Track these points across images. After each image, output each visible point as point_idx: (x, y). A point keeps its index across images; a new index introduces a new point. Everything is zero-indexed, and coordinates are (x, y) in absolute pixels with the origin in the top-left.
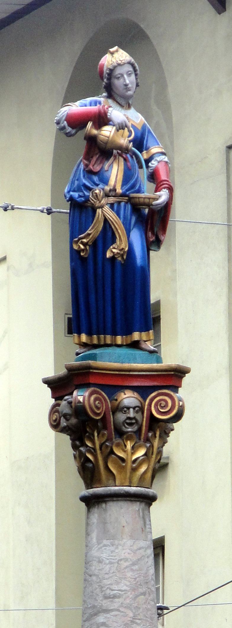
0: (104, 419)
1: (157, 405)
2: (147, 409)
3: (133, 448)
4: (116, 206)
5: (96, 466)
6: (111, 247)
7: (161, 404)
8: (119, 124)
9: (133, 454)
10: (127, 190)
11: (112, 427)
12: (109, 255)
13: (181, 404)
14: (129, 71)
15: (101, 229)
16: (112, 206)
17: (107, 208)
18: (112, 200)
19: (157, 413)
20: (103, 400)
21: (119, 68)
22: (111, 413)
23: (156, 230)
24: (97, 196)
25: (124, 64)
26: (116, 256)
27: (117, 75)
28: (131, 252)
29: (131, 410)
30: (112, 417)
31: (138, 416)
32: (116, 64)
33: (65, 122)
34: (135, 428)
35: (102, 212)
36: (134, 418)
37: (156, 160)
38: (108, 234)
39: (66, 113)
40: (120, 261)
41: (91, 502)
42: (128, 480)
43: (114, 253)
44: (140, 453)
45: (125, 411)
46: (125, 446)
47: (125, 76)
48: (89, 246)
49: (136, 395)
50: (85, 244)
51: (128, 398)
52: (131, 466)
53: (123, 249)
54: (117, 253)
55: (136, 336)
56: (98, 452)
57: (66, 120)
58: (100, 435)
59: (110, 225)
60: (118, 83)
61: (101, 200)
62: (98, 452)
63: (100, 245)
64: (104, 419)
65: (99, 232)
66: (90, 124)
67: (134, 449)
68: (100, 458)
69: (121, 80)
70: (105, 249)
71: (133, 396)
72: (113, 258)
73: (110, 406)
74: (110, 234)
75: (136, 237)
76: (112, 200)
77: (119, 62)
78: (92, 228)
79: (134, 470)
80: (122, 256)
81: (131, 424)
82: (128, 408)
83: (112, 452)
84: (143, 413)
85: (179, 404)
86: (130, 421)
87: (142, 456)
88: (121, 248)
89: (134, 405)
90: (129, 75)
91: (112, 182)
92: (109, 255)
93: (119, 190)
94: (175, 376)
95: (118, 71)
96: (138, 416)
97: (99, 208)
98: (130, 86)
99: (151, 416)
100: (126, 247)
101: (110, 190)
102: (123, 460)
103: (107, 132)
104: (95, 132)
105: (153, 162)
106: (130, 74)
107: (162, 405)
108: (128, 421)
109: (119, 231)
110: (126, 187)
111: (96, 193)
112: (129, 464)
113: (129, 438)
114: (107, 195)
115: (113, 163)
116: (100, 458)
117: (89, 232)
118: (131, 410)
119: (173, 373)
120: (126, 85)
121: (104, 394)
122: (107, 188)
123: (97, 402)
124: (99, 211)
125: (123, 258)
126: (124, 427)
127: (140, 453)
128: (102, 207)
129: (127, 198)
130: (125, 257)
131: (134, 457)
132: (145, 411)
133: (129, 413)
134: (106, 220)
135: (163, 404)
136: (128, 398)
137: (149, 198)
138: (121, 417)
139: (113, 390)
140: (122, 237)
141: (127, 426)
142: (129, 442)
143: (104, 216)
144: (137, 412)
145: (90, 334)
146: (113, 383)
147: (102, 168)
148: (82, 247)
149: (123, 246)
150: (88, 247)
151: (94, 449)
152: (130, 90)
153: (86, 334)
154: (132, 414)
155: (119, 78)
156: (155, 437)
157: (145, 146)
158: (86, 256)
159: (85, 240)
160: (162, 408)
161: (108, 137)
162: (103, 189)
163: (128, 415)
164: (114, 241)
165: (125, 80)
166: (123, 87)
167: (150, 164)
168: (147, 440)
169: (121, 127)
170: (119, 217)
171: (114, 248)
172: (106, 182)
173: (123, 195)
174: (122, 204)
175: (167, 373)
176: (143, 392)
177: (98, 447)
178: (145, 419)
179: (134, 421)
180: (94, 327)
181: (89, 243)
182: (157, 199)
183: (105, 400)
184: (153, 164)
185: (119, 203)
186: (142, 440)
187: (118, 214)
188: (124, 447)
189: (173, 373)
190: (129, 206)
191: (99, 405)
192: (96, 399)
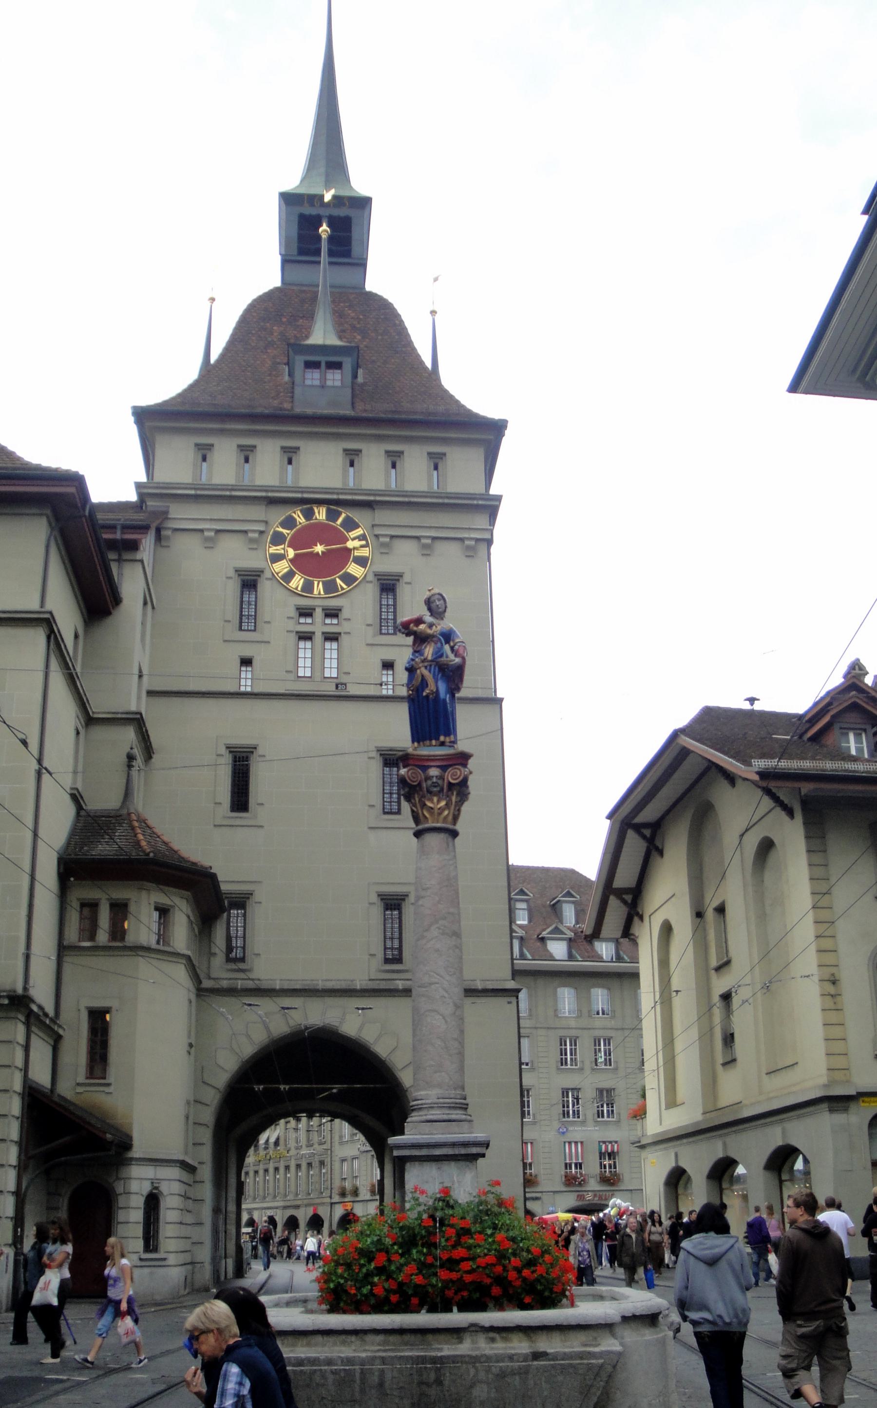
0: (420, 784)
5: (418, 814)
12: (424, 694)
16: (426, 667)
18: (426, 664)
31: (440, 782)
44: (443, 803)
60: (433, 606)
64: (420, 784)
66: (412, 625)
67: (439, 802)
70: (423, 691)
76: (426, 664)
79: (440, 814)
81: (435, 787)
83: (425, 805)
86: (435, 785)
90: (439, 600)
91: (426, 654)
92: (424, 694)
93: (430, 658)
95: (432, 599)
96: (440, 782)
102: (432, 808)
103: (422, 627)
112: (436, 811)
124: (418, 671)
127: (443, 803)
128: (420, 668)
131: (439, 806)
134: (423, 676)
138: (429, 782)
139: (425, 768)
146: (422, 764)
154: (434, 780)
168: (448, 796)
169: (431, 626)
172: (422, 655)
173: (431, 661)
176: (444, 768)
184: (456, 647)
185: (431, 666)
187: (430, 671)
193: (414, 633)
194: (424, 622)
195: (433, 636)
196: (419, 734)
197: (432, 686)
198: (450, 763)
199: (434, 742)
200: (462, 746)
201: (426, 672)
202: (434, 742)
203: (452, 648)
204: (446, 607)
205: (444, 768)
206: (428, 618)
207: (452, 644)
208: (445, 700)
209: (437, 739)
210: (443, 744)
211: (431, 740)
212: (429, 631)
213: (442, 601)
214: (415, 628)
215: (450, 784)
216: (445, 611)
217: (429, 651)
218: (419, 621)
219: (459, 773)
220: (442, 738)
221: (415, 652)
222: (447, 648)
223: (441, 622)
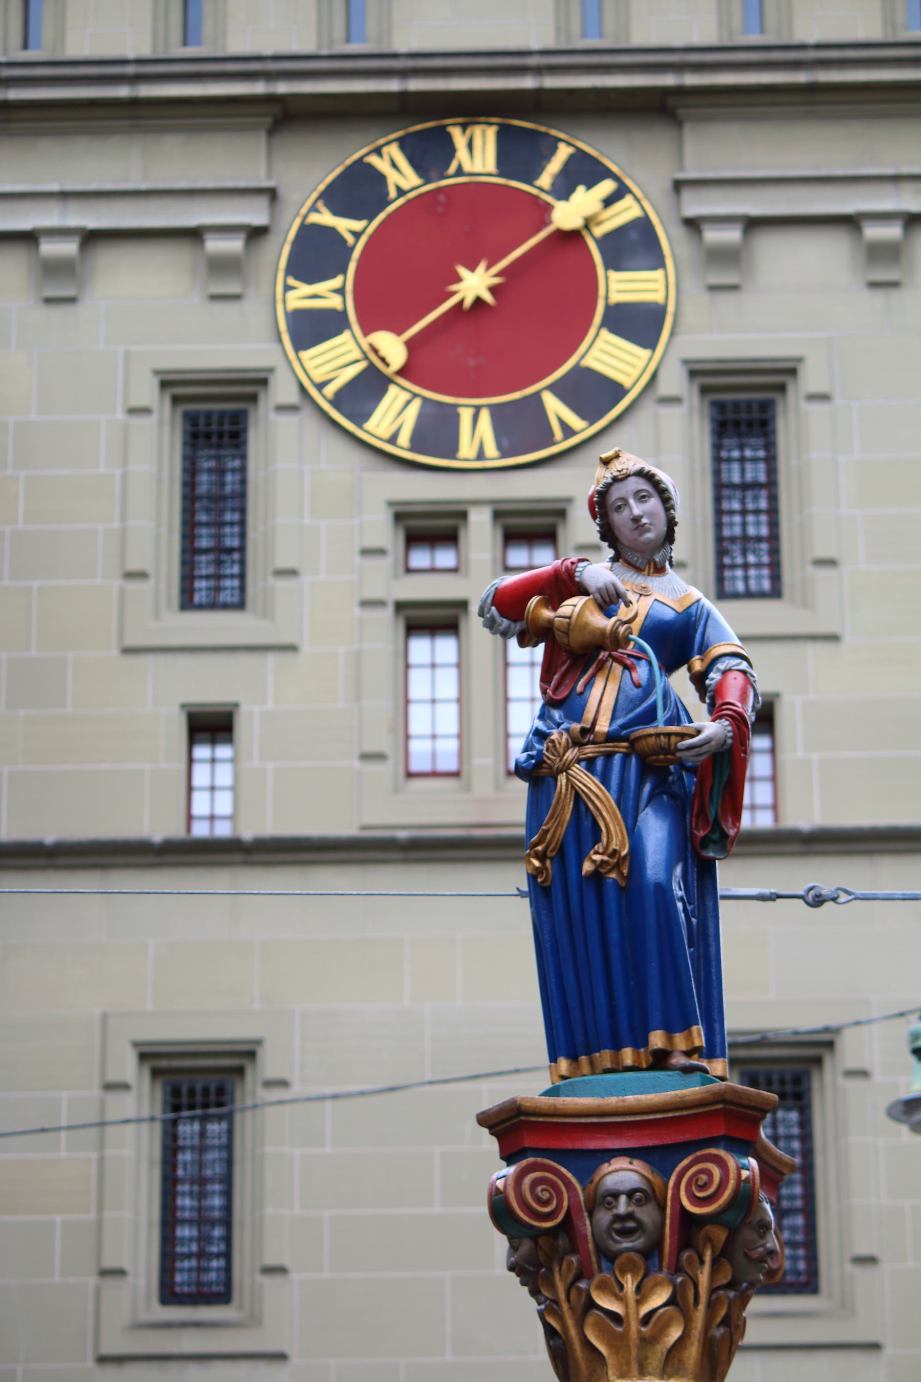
2: (673, 1195)
3: (638, 1289)
4: (599, 763)
6: (592, 852)
7: (697, 1181)
8: (599, 590)
9: (639, 1303)
10: (623, 727)
11: (591, 1246)
12: (587, 867)
13: (743, 1177)
14: (640, 491)
15: (568, 816)
16: (590, 764)
17: (578, 771)
18: (589, 750)
19: (693, 1204)
20: (560, 1183)
21: (616, 486)
22: (586, 1214)
23: (712, 813)
24: (554, 746)
25: (627, 476)
26: (603, 871)
27: (614, 503)
29: (623, 1199)
30: (588, 1223)
31: (647, 1214)
32: (610, 480)
33: (493, 608)
34: (638, 1242)
35: (568, 780)
36: (630, 1216)
37: (719, 670)
39: (493, 589)
40: (614, 879)
42: (634, 1366)
43: (594, 862)
44: (659, 1298)
45: (609, 1203)
46: (621, 1287)
47: (632, 501)
48: (551, 859)
49: (638, 1165)
50: (542, 857)
51: (622, 1174)
52: (639, 1332)
53: (615, 852)
54: (602, 861)
55: (657, 1039)
56: (565, 1306)
57: (494, 603)
58: (564, 1267)
59: (587, 808)
60: (620, 519)
61: (564, 755)
62: (565, 1306)
63: (571, 850)
64: (567, 1225)
65: (565, 825)
67: (642, 1293)
68: (570, 1323)
69: (625, 513)
70: (581, 857)
71: (630, 1167)
72: (597, 876)
73: (582, 1198)
74: (587, 823)
76: (589, 750)
77: (615, 474)
78: (550, 819)
79: (648, 1342)
80: (617, 866)
81: (626, 1233)
82: (616, 1195)
83: (591, 1305)
84: (662, 1208)
85: (739, 1175)
86: (626, 1226)
87: (664, 1305)
88: (610, 850)
89: (628, 1186)
90: (641, 497)
91: (589, 715)
92: (587, 867)
93: (603, 726)
95: (616, 493)
96: (647, 1214)
97: (560, 771)
98: (644, 520)
99: (683, 1208)
100: (623, 845)
101: (584, 732)
104: (547, 613)
105: (712, 675)
106: (644, 497)
107: (700, 1183)
108: (617, 1226)
109: (604, 813)
110: (620, 721)
111: (553, 741)
112: (634, 1326)
113: (629, 1267)
115: (594, 676)
116: (570, 1323)
117: (544, 827)
118: (623, 1199)
119: (720, 1106)
120: (636, 520)
121: (564, 1170)
122: (576, 727)
123: (539, 1188)
124: (562, 778)
125: (620, 873)
126: (610, 1242)
127: (659, 1298)
128: (566, 768)
129: (625, 744)
130: (625, 871)
131: (644, 1310)
132: (669, 1203)
133: (616, 1207)
135: (704, 1177)
136: (622, 1174)
137: (668, 735)
138: (604, 1217)
139: (587, 1162)
140: (611, 826)
141: (617, 1238)
142: (629, 1277)
143: (573, 787)
144: (639, 1203)
147: (574, 688)
148: (536, 863)
149: (614, 845)
150: (548, 863)
151: (556, 1302)
152: (648, 530)
153: (568, 1057)
154: (622, 1206)
155: (619, 507)
156: (702, 1262)
157: (696, 647)
158: (548, 884)
159: (540, 848)
160: (702, 1188)
161: (569, 618)
162: (567, 730)
163: (615, 1211)
164: (597, 839)
165: (631, 509)
166: (631, 525)
167: (708, 682)
168: (677, 1269)
170: (608, 788)
171: (597, 853)
172: (577, 716)
173: (610, 737)
174: (617, 757)
175: (706, 1109)
176: (660, 1158)
177: (562, 1296)
178: (668, 1222)
179: (631, 1224)
180: (580, 1038)
181: (549, 854)
182: (692, 736)
183: (568, 1184)
185: (609, 756)
186: (665, 1270)
188: (617, 1289)
189: (720, 1106)
190: (634, 760)
191: (545, 1196)
192: (535, 1183)
194: (581, 590)
195: (615, 641)
196: (574, 1028)
197: (615, 835)
198: (680, 1138)
199: (628, 1055)
201: (588, 782)
202: (628, 1055)
203: (699, 680)
204: (671, 523)
207: (698, 665)
208: (663, 890)
209: (640, 1042)
210: (660, 1061)
211: (617, 1047)
212: (599, 621)
213: (654, 503)
214: (547, 613)
215: (687, 1221)
216: (669, 537)
217: (602, 698)
219: (717, 1172)
220: (657, 1039)
221: (550, 703)
222: (680, 683)
223: (654, 583)
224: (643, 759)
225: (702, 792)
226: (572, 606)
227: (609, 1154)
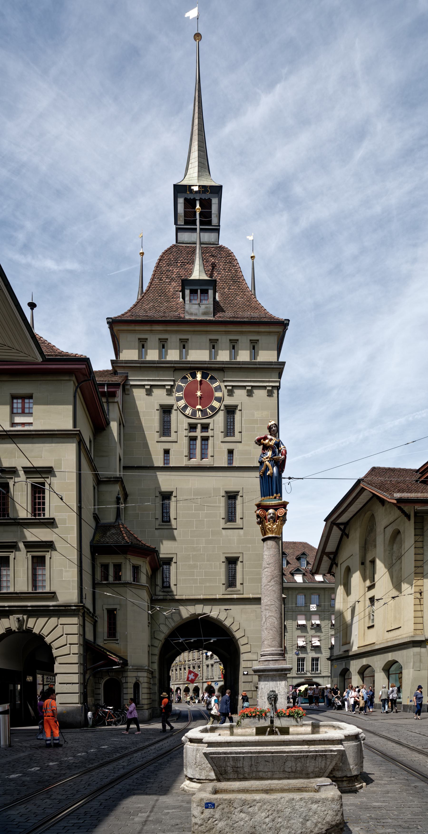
1: (280, 512)
12: (267, 474)
16: (268, 461)
17: (267, 462)
28: (273, 473)
38: (267, 469)
41: (264, 540)
44: (275, 526)
72: (269, 475)
75: (275, 469)
76: (268, 459)
90: (274, 427)
92: (267, 474)
93: (270, 456)
94: (284, 505)
114: (267, 458)
136: (271, 511)
145: (264, 497)
154: (272, 515)
172: (267, 455)
173: (271, 458)
176: (276, 510)
193: (263, 444)
199: (271, 497)
200: (284, 499)
205: (276, 510)
206: (269, 437)
209: (272, 495)
211: (270, 496)
218: (265, 438)
224: (275, 461)
225: (281, 465)
226: (267, 441)
227: (270, 509)
